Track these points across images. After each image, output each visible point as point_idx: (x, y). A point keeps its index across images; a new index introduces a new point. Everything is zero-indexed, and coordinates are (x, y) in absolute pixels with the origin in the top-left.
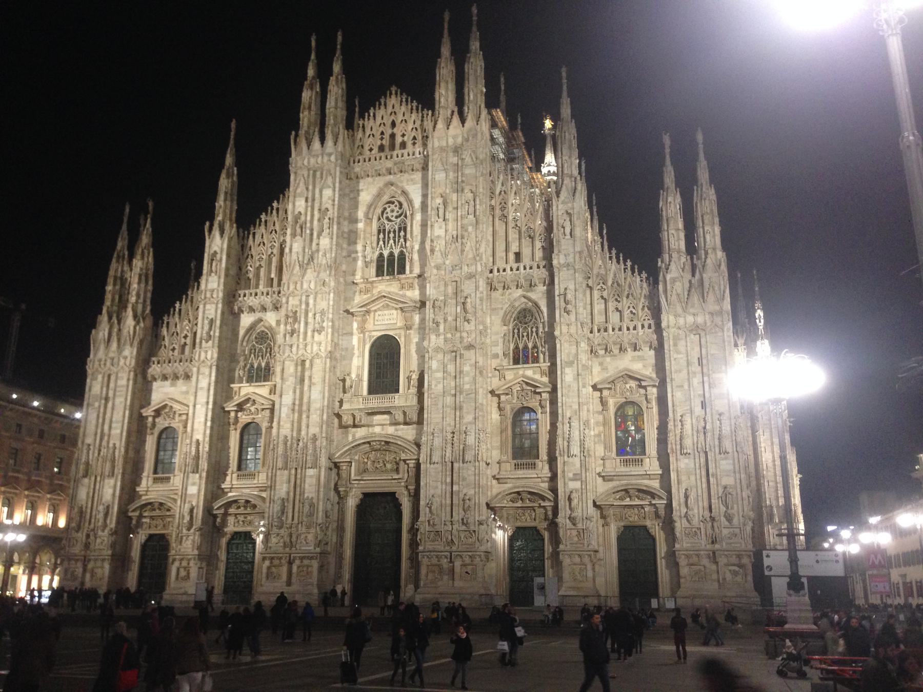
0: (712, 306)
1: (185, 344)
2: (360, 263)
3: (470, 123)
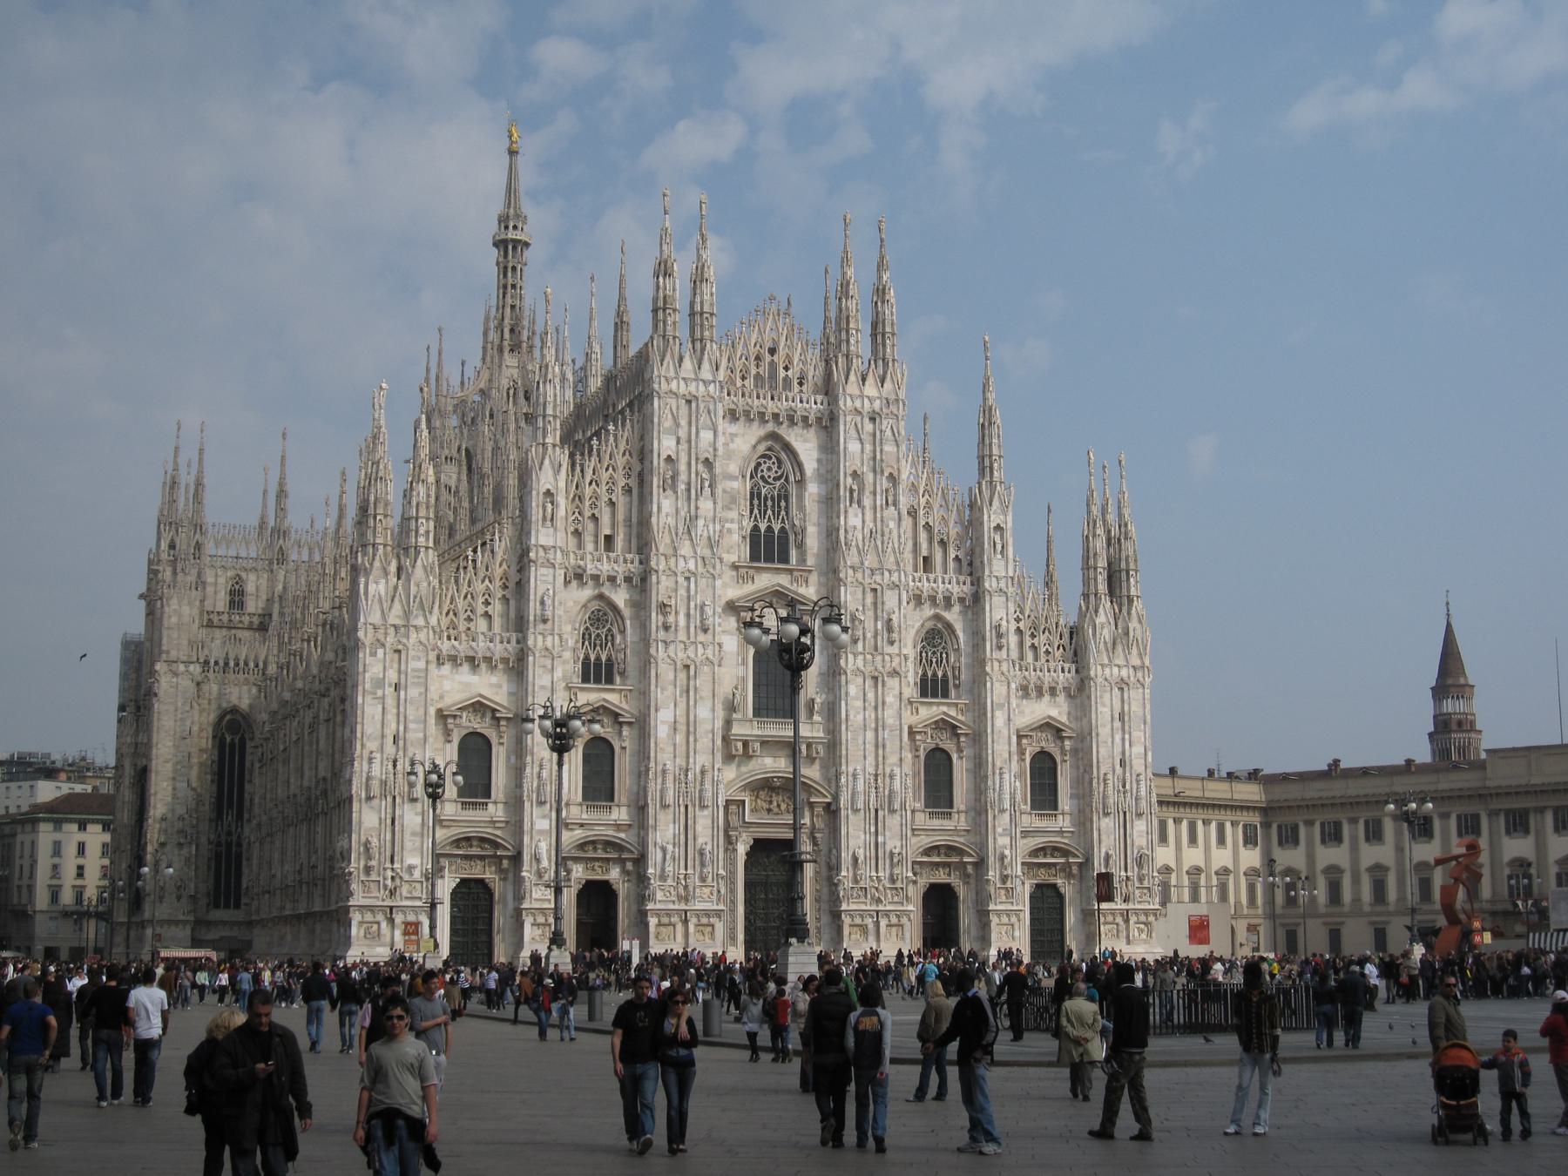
0: (1135, 661)
2: (736, 537)
3: (888, 385)
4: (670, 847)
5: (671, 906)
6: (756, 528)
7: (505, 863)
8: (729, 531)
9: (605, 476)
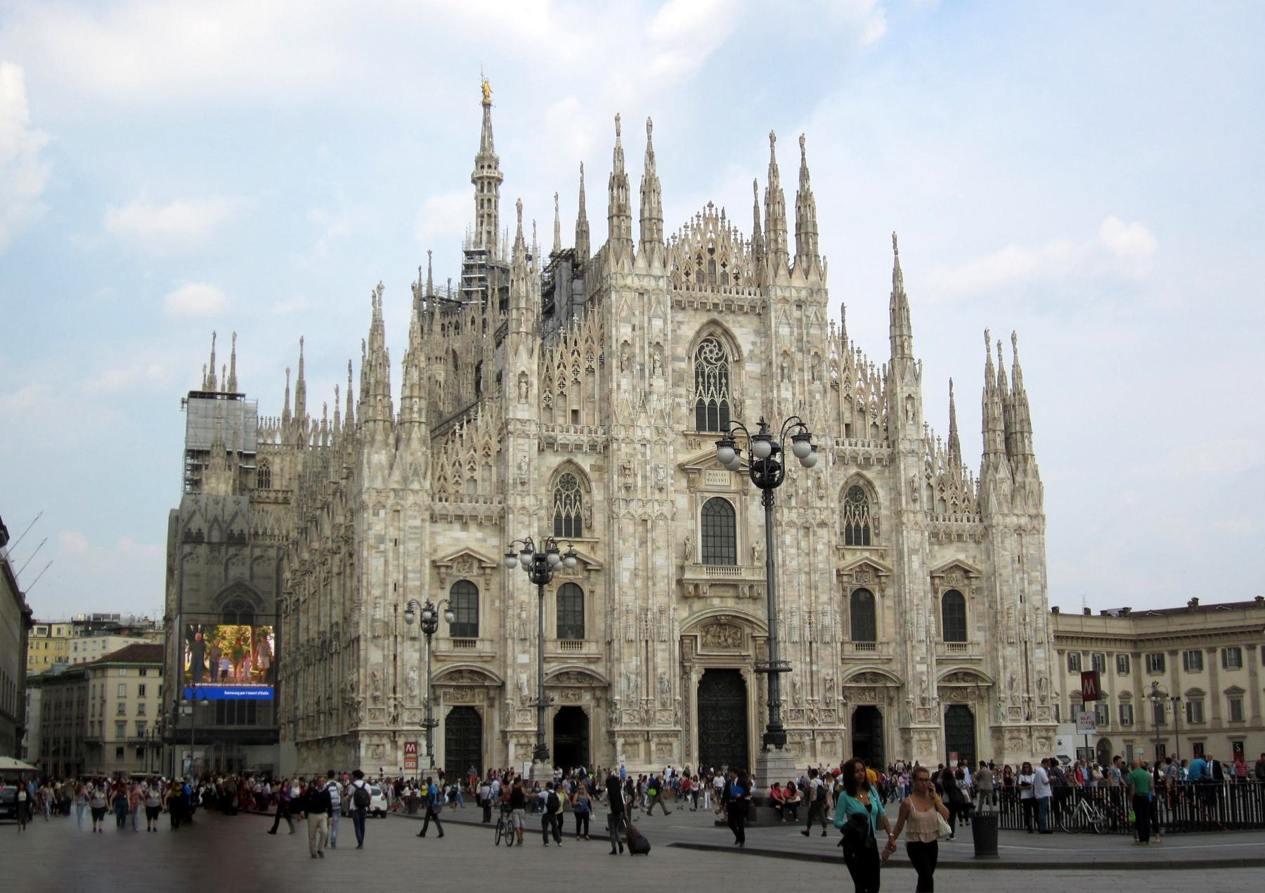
4: (633, 677)
5: (636, 728)
6: (701, 402)
7: (492, 693)
8: (678, 404)
9: (572, 359)
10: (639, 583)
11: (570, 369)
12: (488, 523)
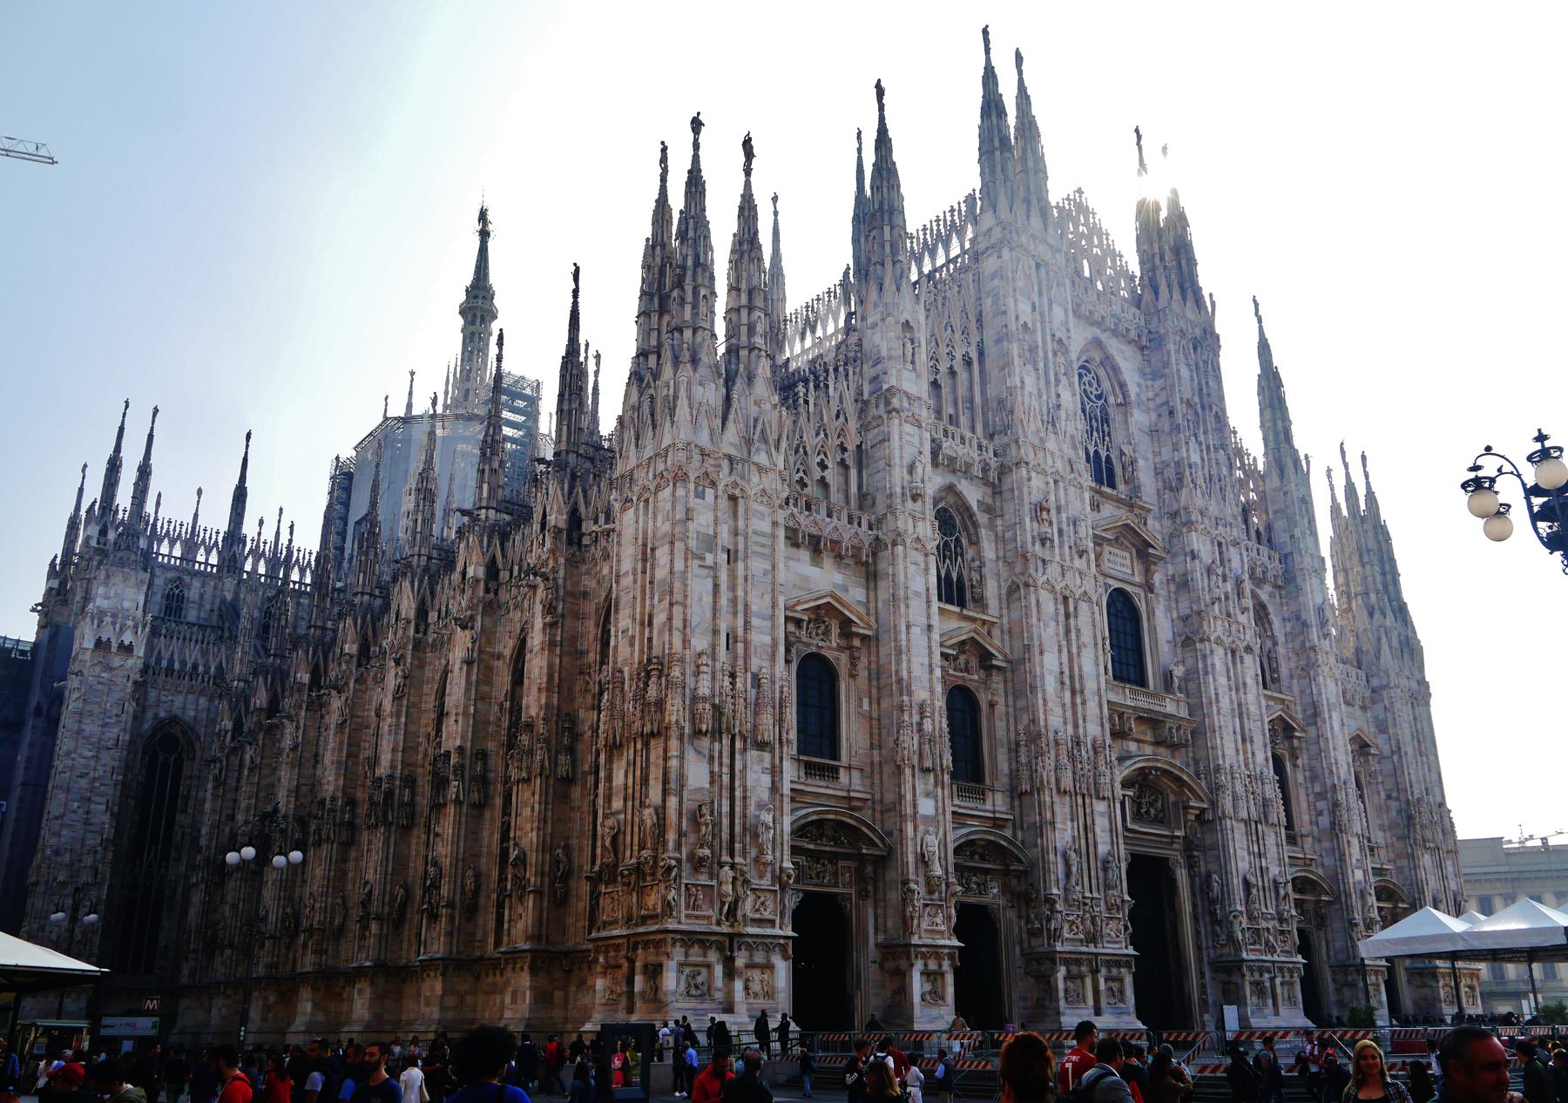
1: (823, 478)
7: (869, 869)
10: (1068, 694)
11: (943, 350)
12: (850, 561)
